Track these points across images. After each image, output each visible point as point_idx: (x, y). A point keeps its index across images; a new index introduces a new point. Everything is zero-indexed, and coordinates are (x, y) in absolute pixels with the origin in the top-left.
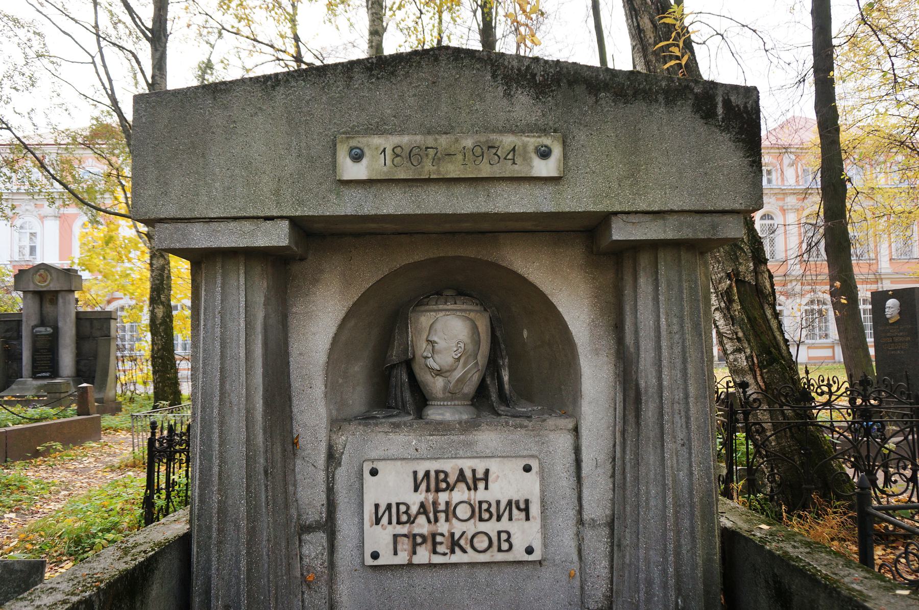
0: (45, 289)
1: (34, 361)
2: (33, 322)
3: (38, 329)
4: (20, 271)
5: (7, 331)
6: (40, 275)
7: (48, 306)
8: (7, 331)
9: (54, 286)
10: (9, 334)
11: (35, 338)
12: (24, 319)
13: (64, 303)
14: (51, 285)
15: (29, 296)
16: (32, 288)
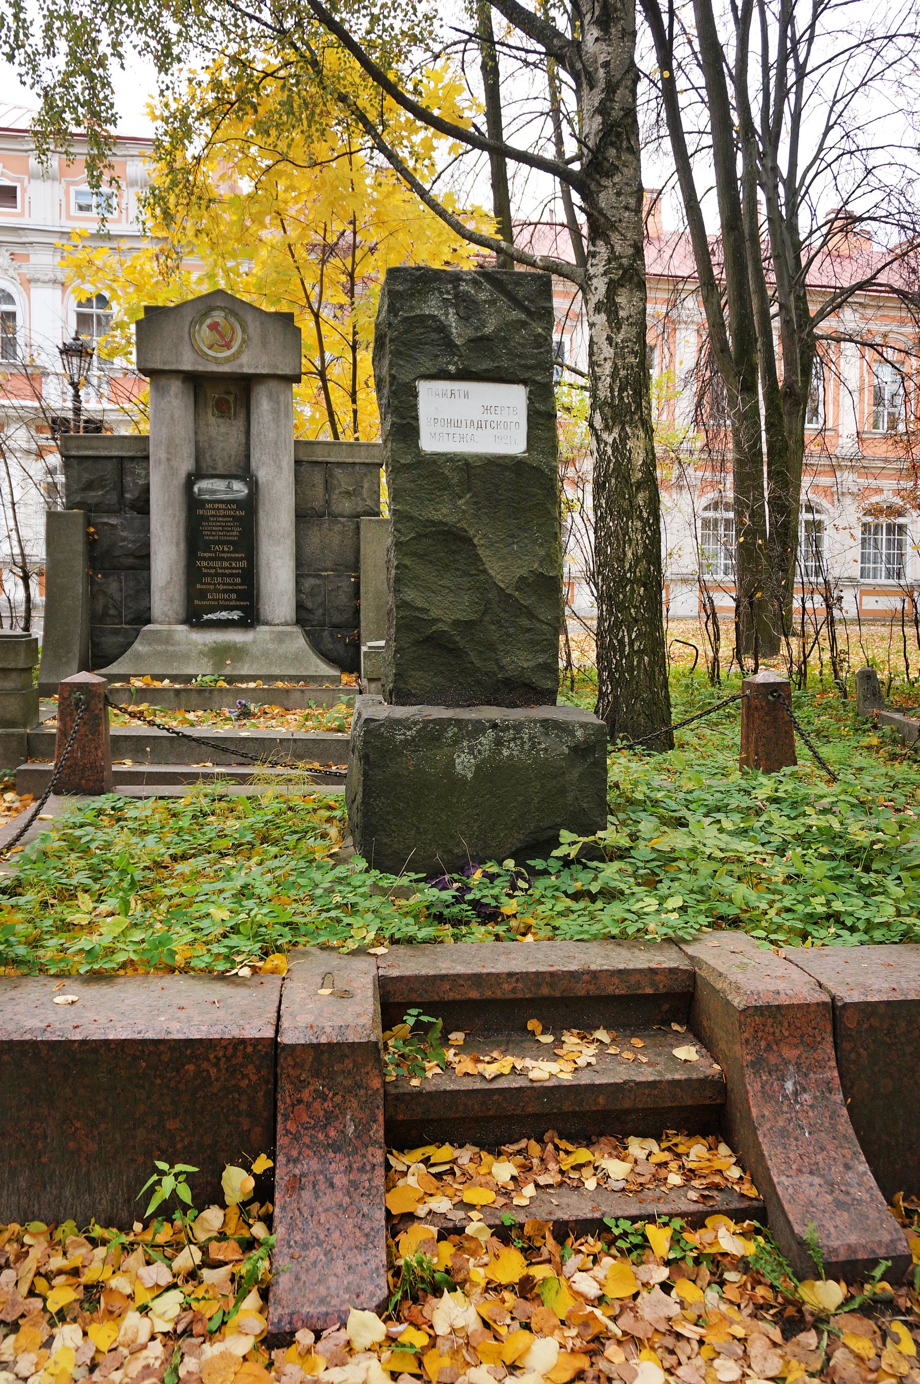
0: (226, 369)
1: (193, 573)
2: (186, 466)
3: (204, 484)
4: (147, 309)
5: (89, 486)
6: (214, 327)
7: (212, 420)
8: (89, 486)
9: (248, 364)
10: (94, 496)
11: (193, 505)
12: (156, 453)
13: (276, 411)
14: (244, 359)
15: (175, 386)
16: (188, 363)
